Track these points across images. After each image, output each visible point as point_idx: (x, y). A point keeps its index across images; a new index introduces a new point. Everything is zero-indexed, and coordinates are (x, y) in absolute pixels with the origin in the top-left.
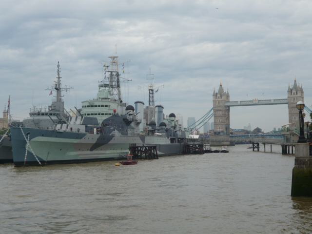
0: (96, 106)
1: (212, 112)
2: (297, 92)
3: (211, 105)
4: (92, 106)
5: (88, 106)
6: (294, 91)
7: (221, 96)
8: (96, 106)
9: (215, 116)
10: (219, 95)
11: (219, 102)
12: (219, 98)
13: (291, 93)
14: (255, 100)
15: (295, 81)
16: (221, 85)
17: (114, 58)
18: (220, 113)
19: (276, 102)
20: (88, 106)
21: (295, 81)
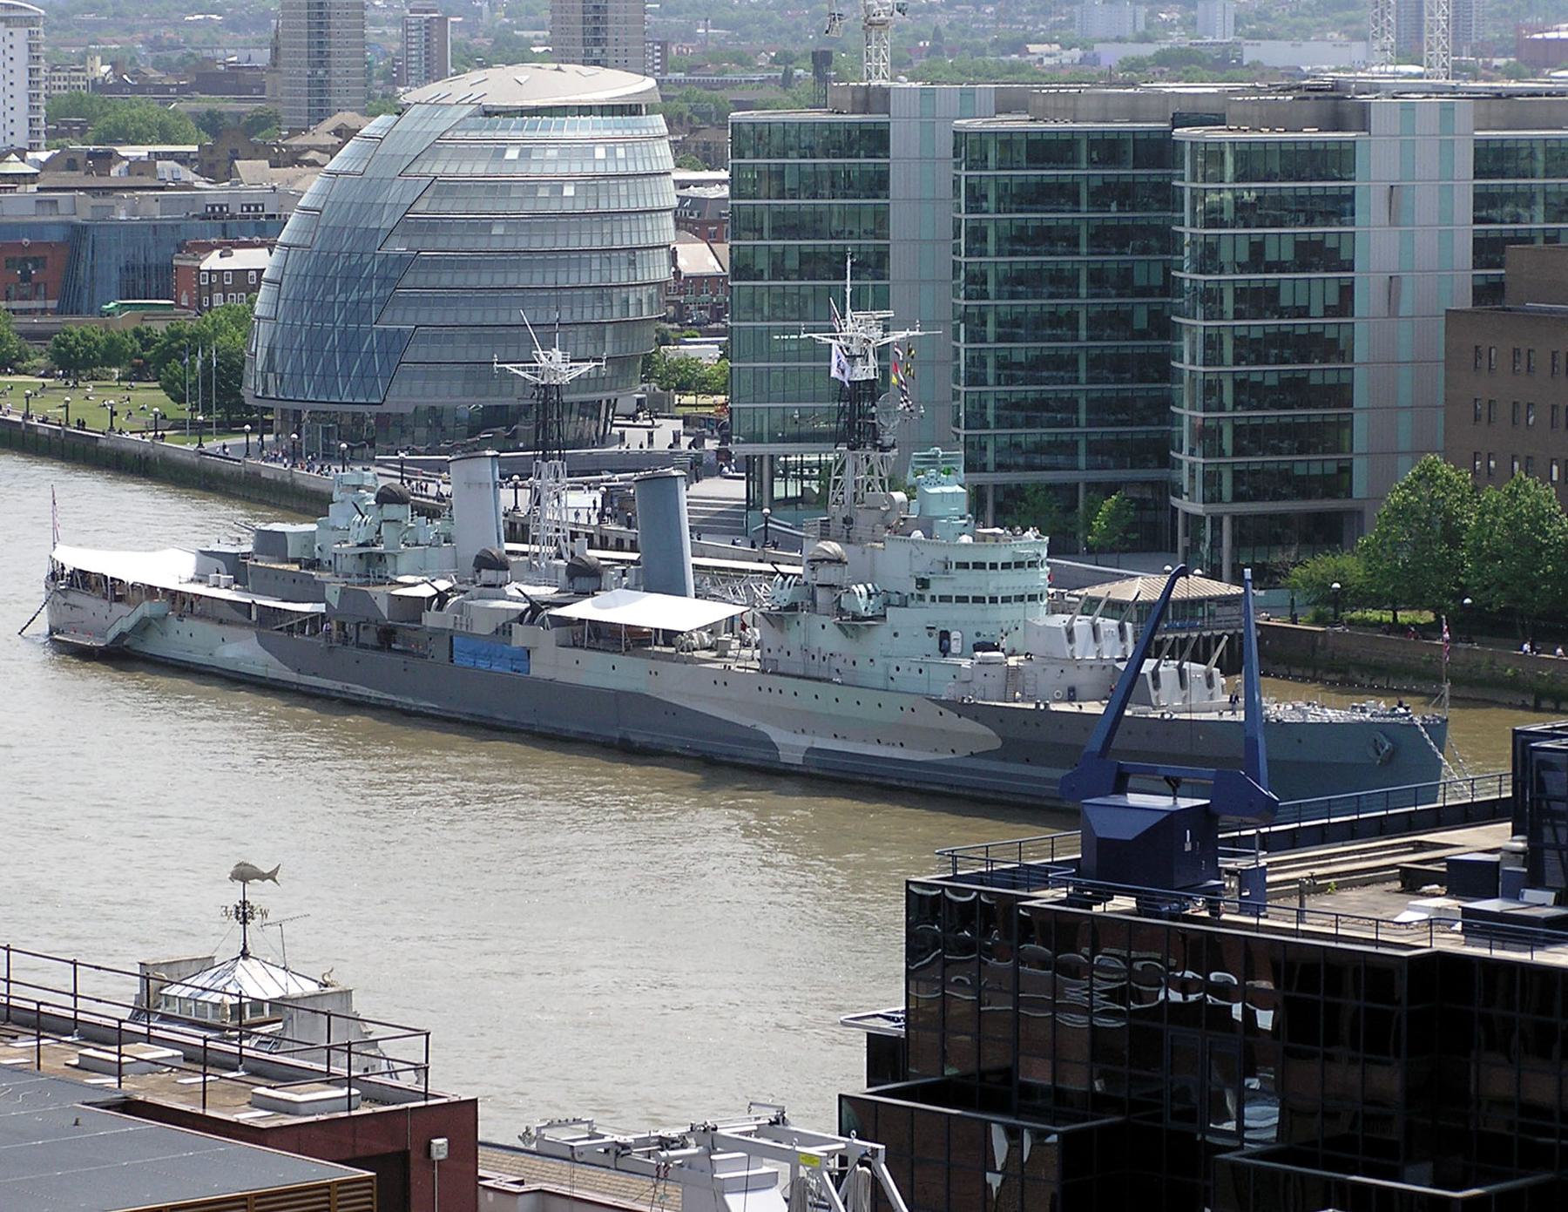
4: (1019, 565)
5: (1006, 566)
20: (1006, 566)
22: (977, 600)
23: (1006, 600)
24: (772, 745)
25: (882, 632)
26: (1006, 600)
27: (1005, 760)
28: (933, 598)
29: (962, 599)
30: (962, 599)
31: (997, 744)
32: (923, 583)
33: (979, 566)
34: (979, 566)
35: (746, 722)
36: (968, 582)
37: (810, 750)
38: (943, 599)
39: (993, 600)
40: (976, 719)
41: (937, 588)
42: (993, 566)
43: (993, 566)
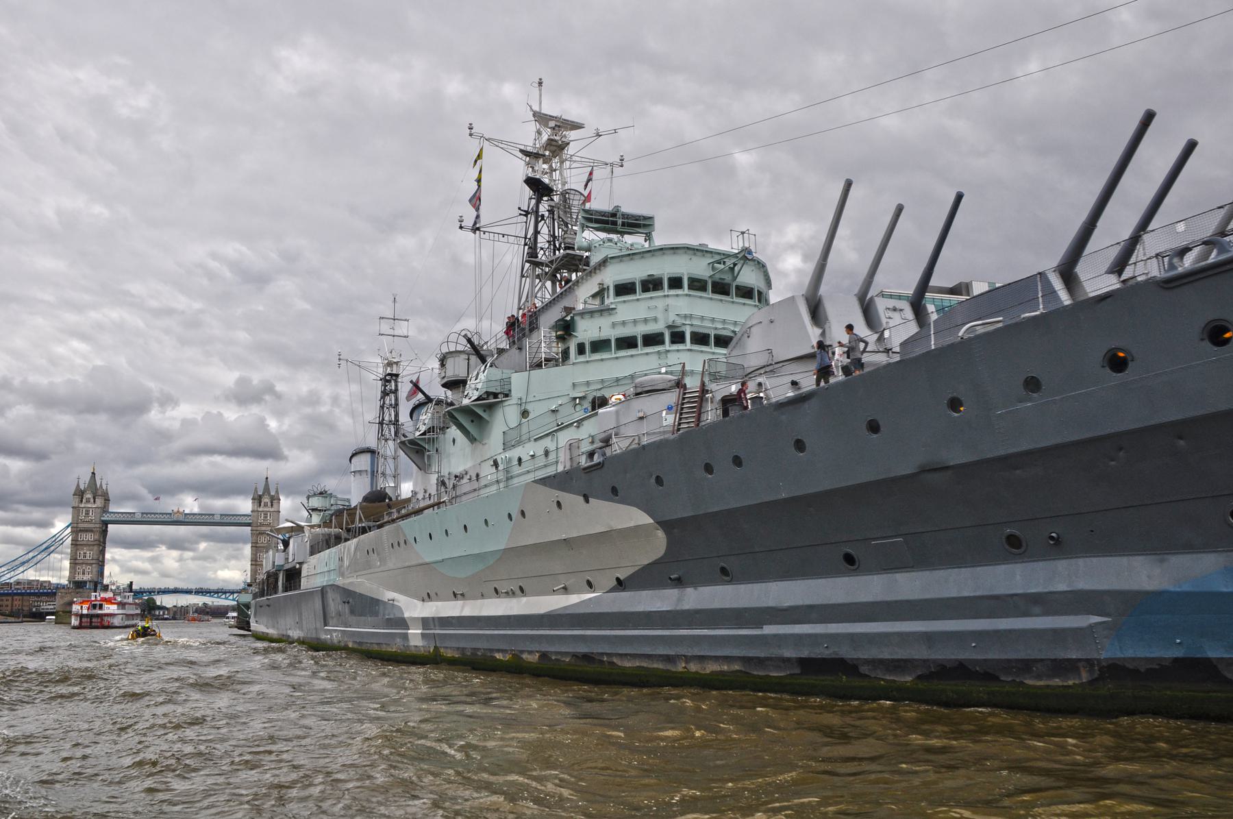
1: (69, 530)
4: (721, 288)
5: (697, 284)
9: (75, 544)
10: (89, 495)
11: (87, 513)
12: (88, 501)
18: (88, 537)
20: (697, 284)
22: (652, 340)
23: (701, 339)
24: (403, 623)
25: (505, 418)
26: (701, 339)
27: (679, 582)
28: (581, 350)
29: (627, 343)
30: (627, 343)
31: (658, 545)
33: (651, 284)
35: (388, 595)
36: (635, 314)
39: (678, 337)
40: (614, 493)
41: (587, 331)
43: (676, 283)
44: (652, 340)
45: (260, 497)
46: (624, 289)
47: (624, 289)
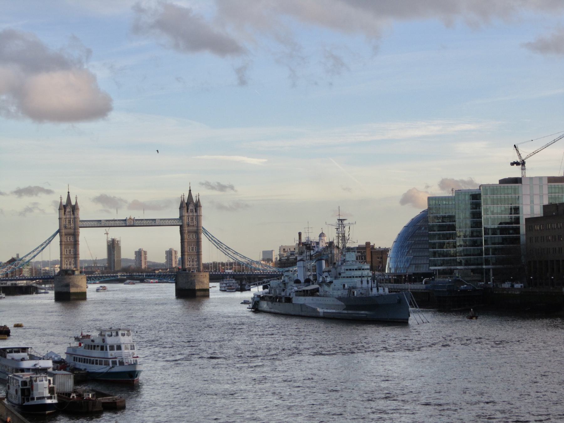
0: (363, 269)
2: (195, 209)
3: (58, 228)
4: (360, 269)
5: (356, 270)
6: (191, 207)
7: (73, 211)
8: (363, 269)
10: (68, 210)
13: (188, 209)
14: (130, 219)
15: (190, 191)
16: (69, 193)
17: (342, 220)
19: (164, 223)
20: (356, 270)
21: (190, 191)
22: (350, 277)
23: (357, 277)
24: (319, 312)
25: (332, 286)
26: (357, 277)
29: (348, 277)
30: (348, 277)
31: (345, 307)
32: (340, 274)
33: (350, 270)
34: (350, 270)
36: (348, 273)
37: (324, 312)
38: (344, 277)
39: (353, 277)
41: (343, 275)
42: (353, 270)
43: (353, 270)
44: (350, 277)
45: (187, 204)
46: (347, 270)
47: (347, 270)
